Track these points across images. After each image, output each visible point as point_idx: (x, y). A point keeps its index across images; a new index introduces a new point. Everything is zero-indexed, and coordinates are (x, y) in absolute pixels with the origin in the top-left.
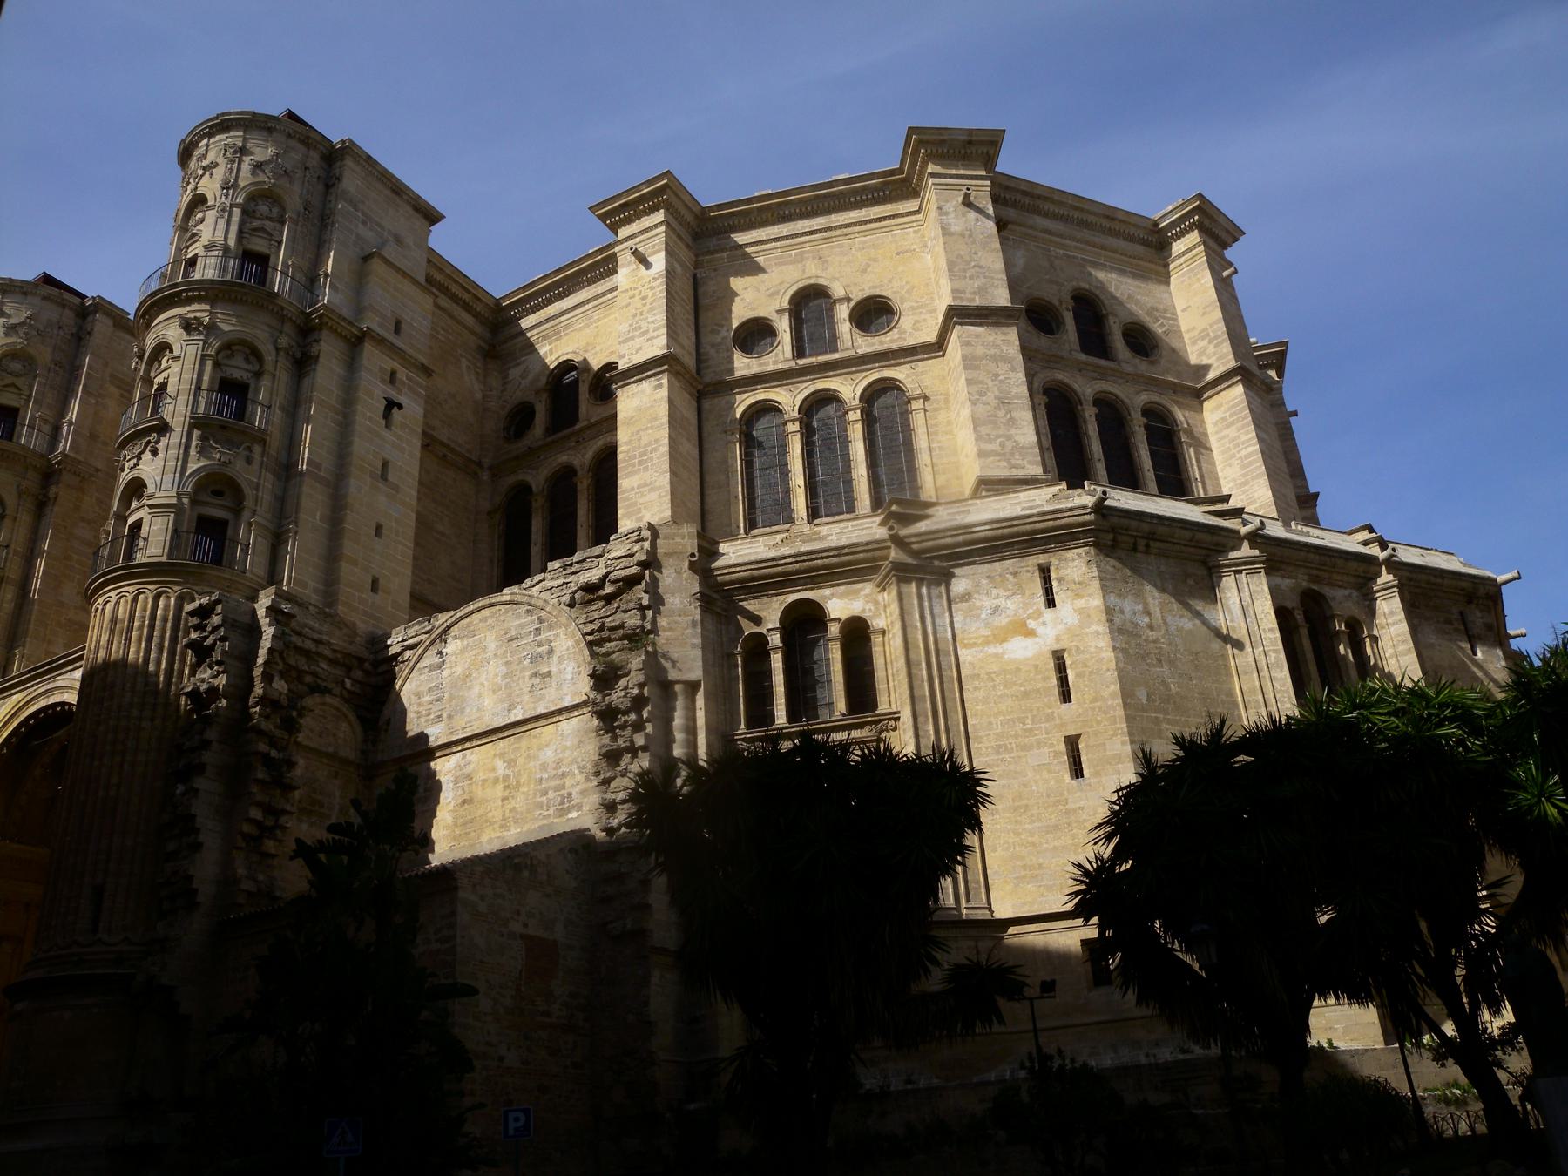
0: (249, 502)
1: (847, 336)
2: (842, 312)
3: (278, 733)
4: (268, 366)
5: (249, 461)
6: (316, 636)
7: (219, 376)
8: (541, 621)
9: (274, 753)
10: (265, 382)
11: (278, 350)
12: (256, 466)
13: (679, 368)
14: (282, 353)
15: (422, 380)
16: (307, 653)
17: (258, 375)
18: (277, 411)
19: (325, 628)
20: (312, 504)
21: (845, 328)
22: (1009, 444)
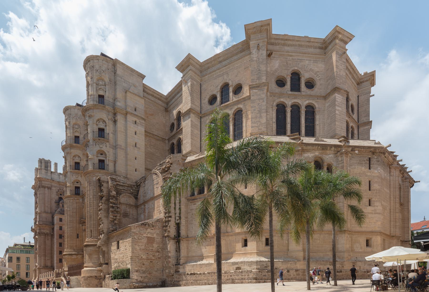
1: (231, 97)
2: (231, 90)
3: (114, 202)
6: (123, 182)
8: (157, 176)
9: (114, 205)
13: (194, 112)
15: (144, 122)
16: (122, 186)
19: (125, 180)
20: (121, 154)
21: (231, 94)
22: (259, 123)
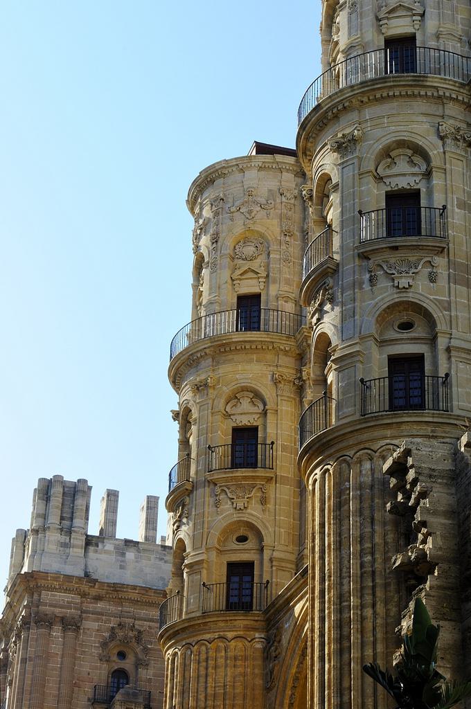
0: (441, 326)
4: (436, 162)
5: (432, 278)
7: (383, 192)
10: (437, 180)
11: (442, 138)
12: (442, 282)
14: (449, 141)
17: (428, 175)
18: (457, 210)
